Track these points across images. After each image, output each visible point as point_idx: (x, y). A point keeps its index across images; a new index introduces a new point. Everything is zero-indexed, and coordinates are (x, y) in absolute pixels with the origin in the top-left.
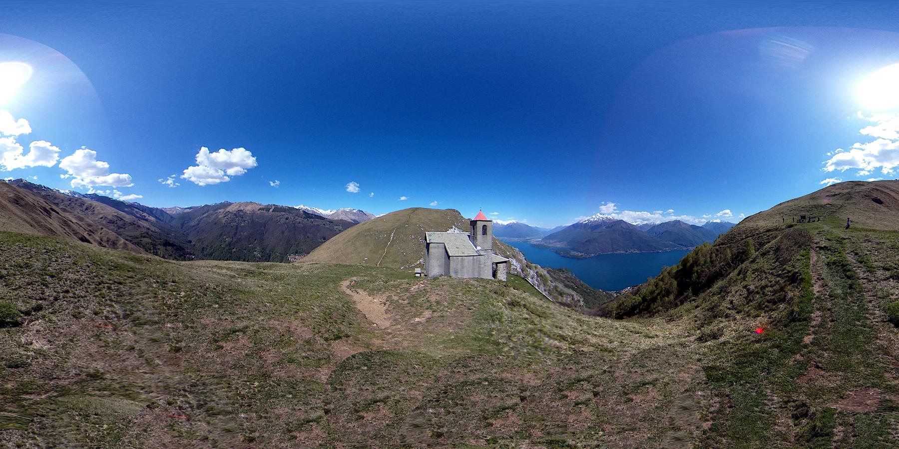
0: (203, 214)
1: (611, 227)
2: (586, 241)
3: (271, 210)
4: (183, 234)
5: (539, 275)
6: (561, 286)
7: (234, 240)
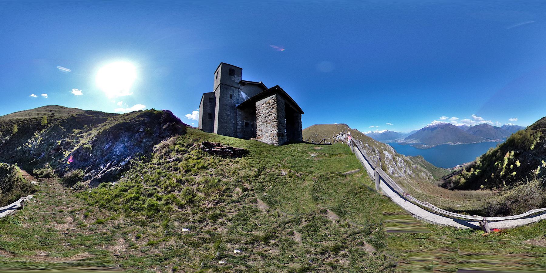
1: (443, 128)
2: (429, 138)
5: (405, 161)
6: (419, 167)
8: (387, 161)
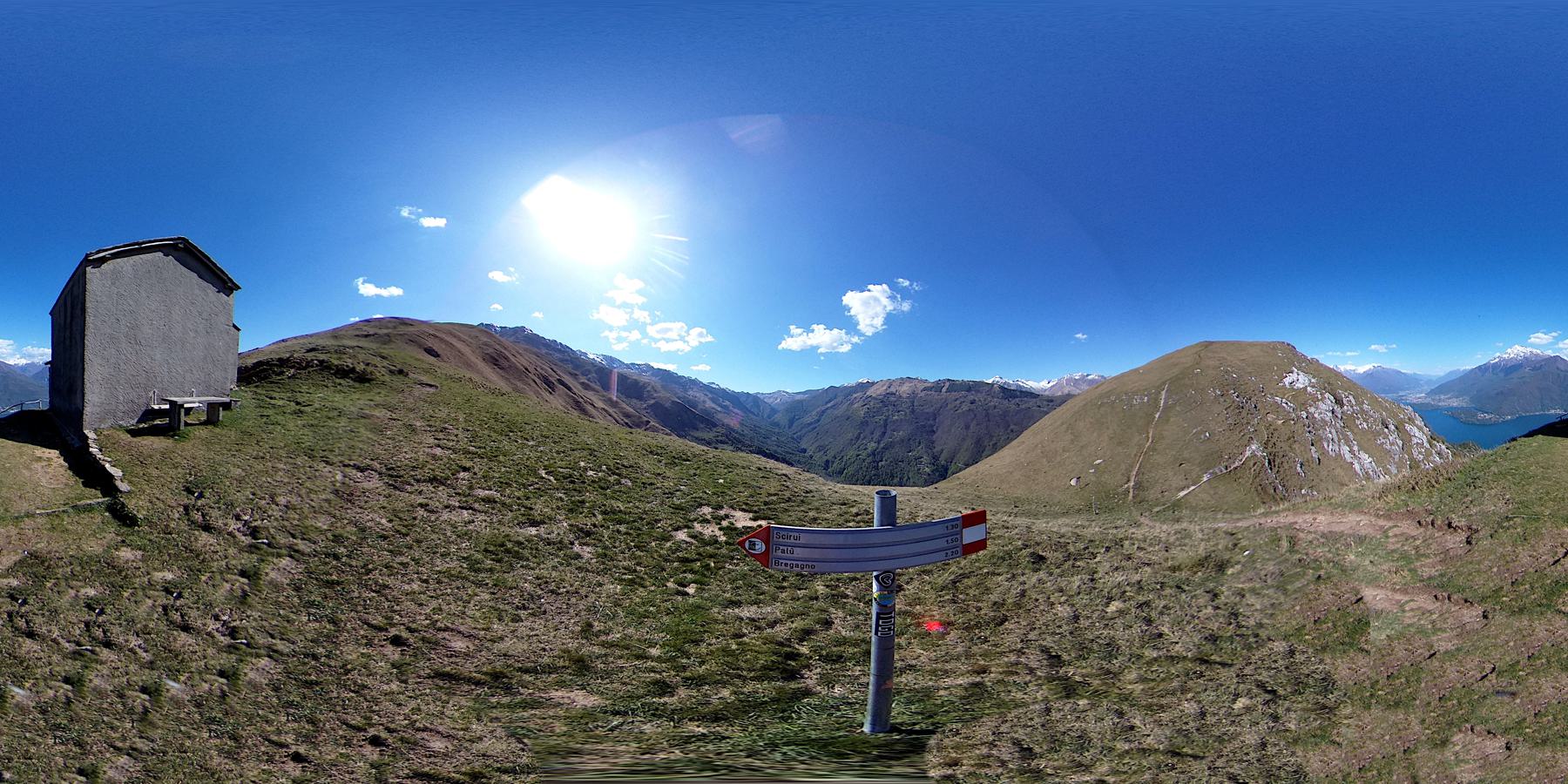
0: (827, 403)
3: (944, 390)
4: (793, 439)
7: (882, 445)
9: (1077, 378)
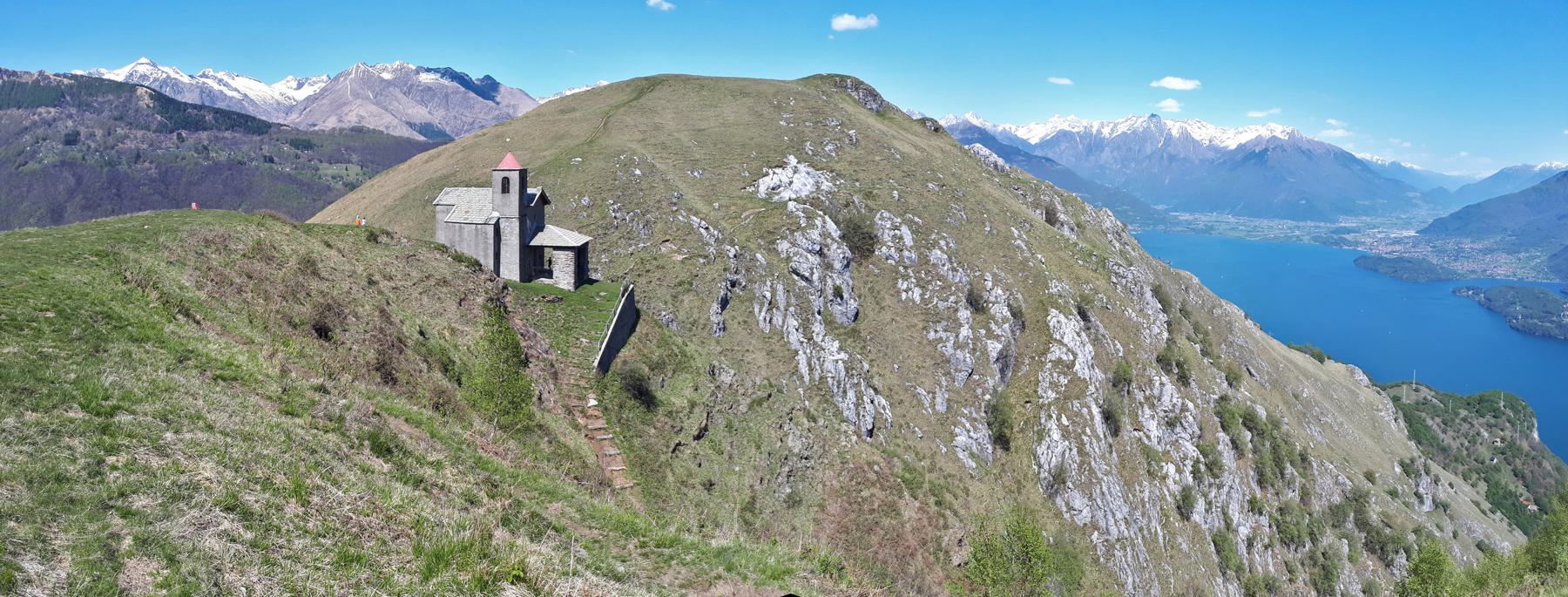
8: (1054, 385)
9: (386, 76)
